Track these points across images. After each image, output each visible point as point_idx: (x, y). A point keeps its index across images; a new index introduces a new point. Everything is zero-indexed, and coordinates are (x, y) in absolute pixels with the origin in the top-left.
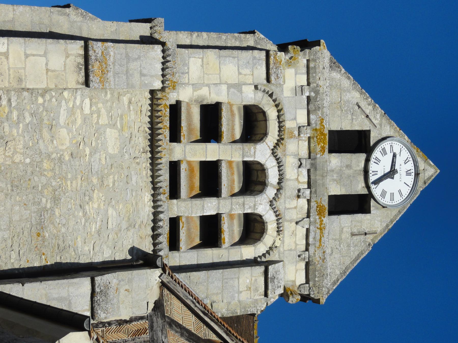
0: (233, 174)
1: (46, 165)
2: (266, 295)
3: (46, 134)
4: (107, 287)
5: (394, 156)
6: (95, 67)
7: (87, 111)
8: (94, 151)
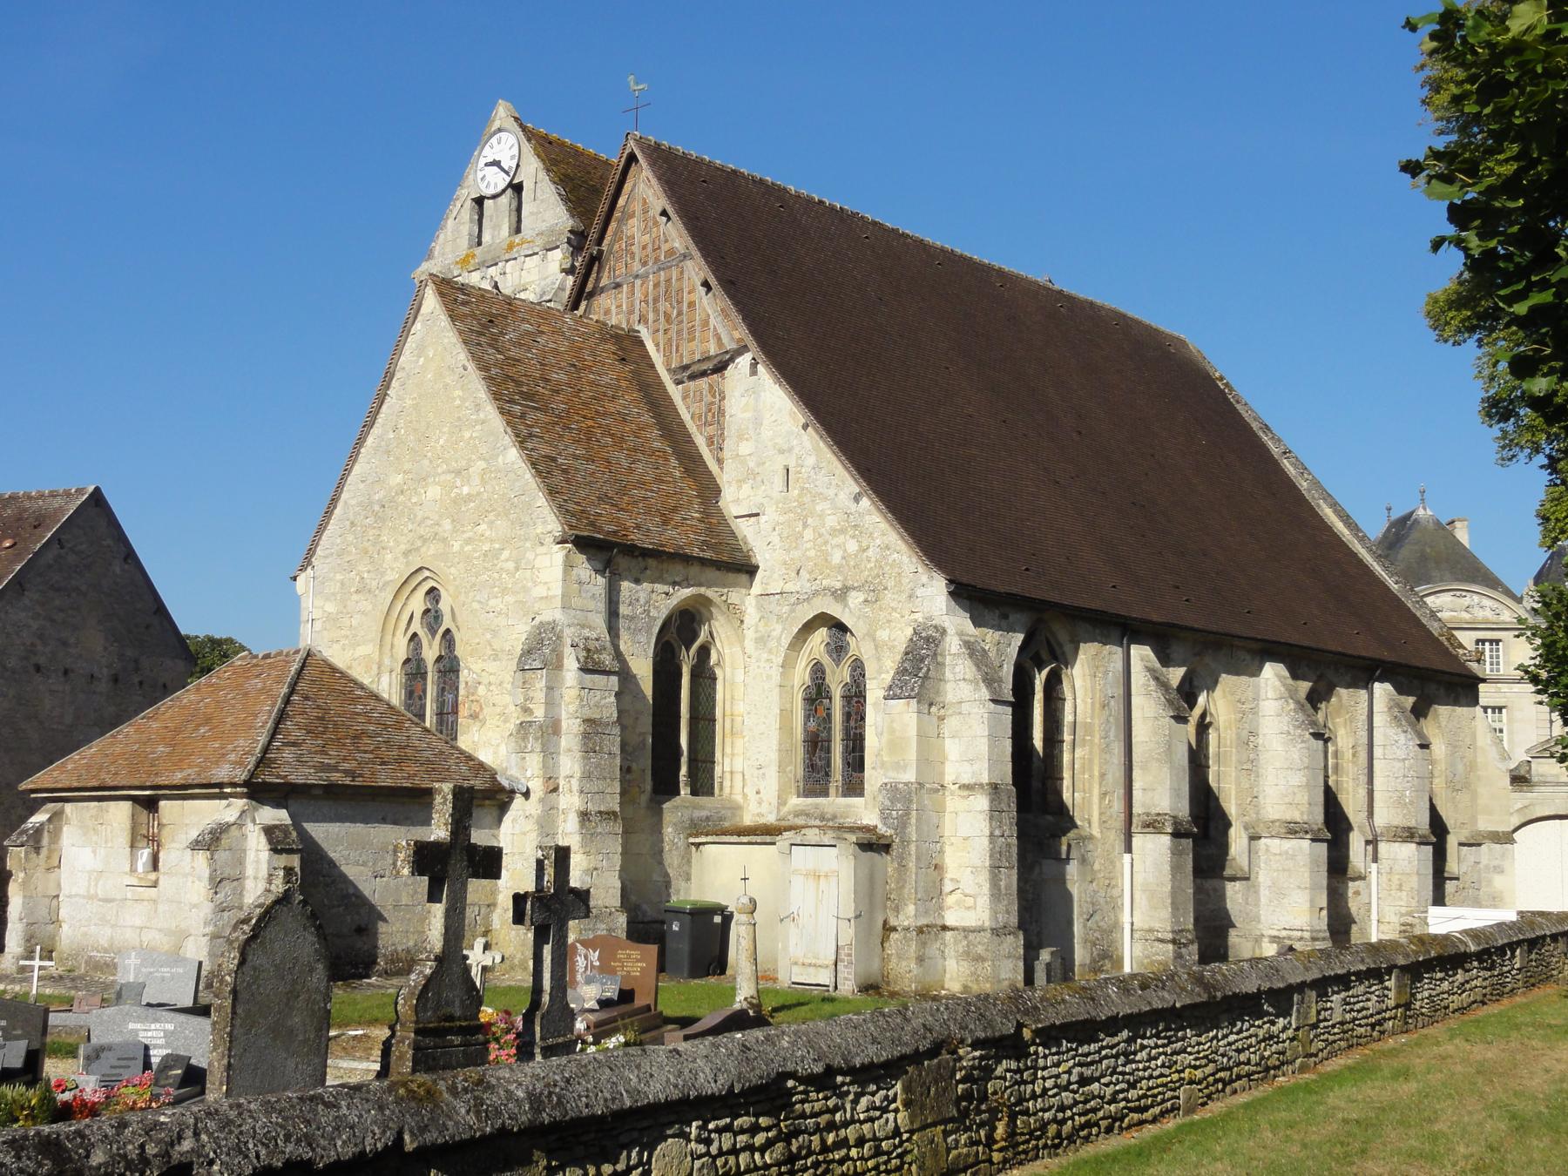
5: (486, 165)
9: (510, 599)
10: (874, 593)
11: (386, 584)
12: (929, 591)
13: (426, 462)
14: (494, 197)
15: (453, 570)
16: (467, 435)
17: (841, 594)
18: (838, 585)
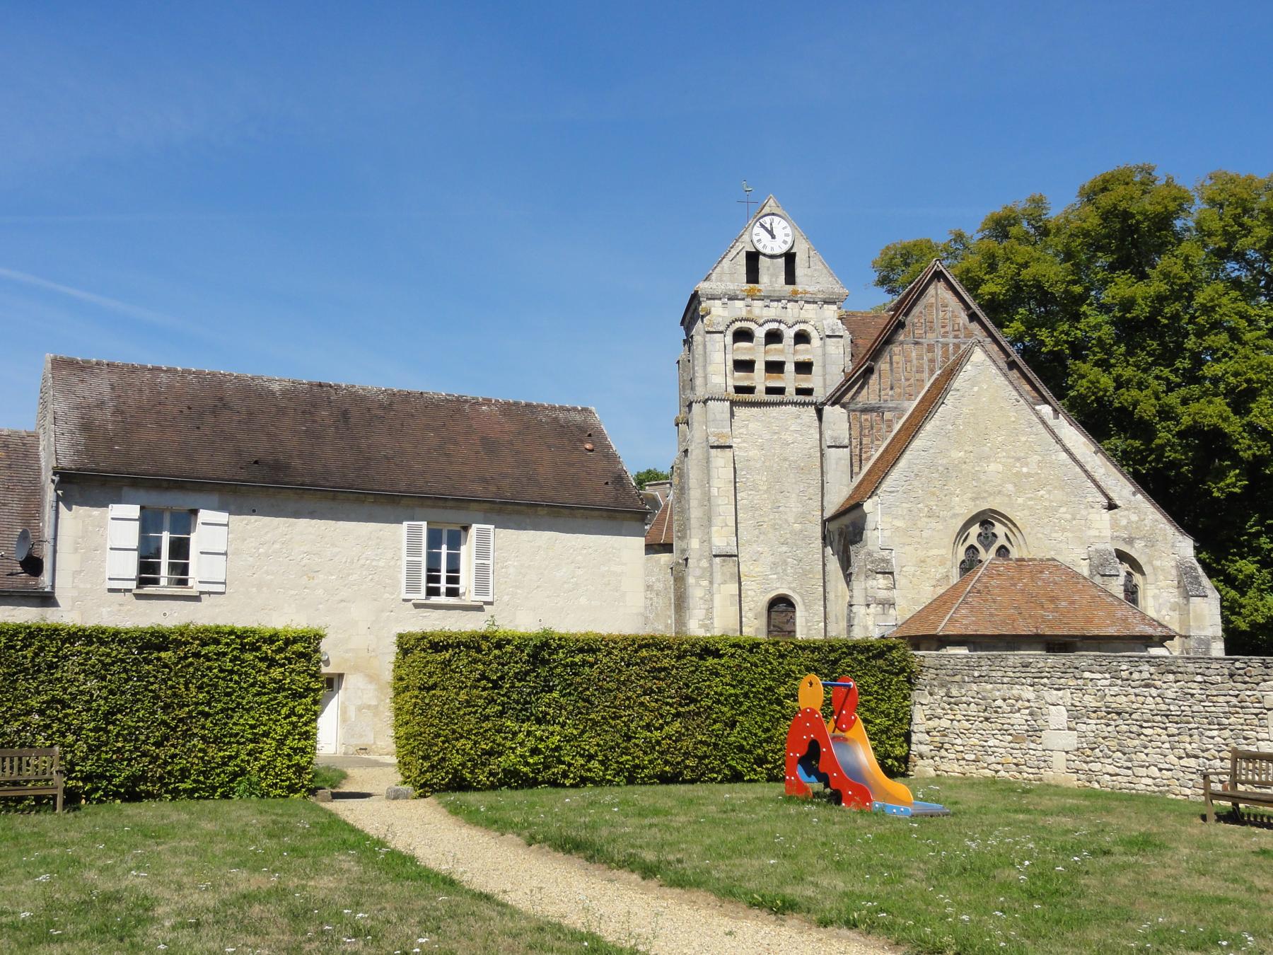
0: (771, 350)
1: (767, 464)
2: (841, 337)
3: (751, 463)
4: (832, 438)
6: (722, 442)
7: (739, 440)
8: (760, 436)
9: (1069, 534)
10: (1151, 542)
11: (955, 516)
12: (1183, 544)
13: (988, 449)
14: (772, 257)
15: (1018, 514)
16: (1023, 439)
17: (1130, 541)
18: (1126, 536)
